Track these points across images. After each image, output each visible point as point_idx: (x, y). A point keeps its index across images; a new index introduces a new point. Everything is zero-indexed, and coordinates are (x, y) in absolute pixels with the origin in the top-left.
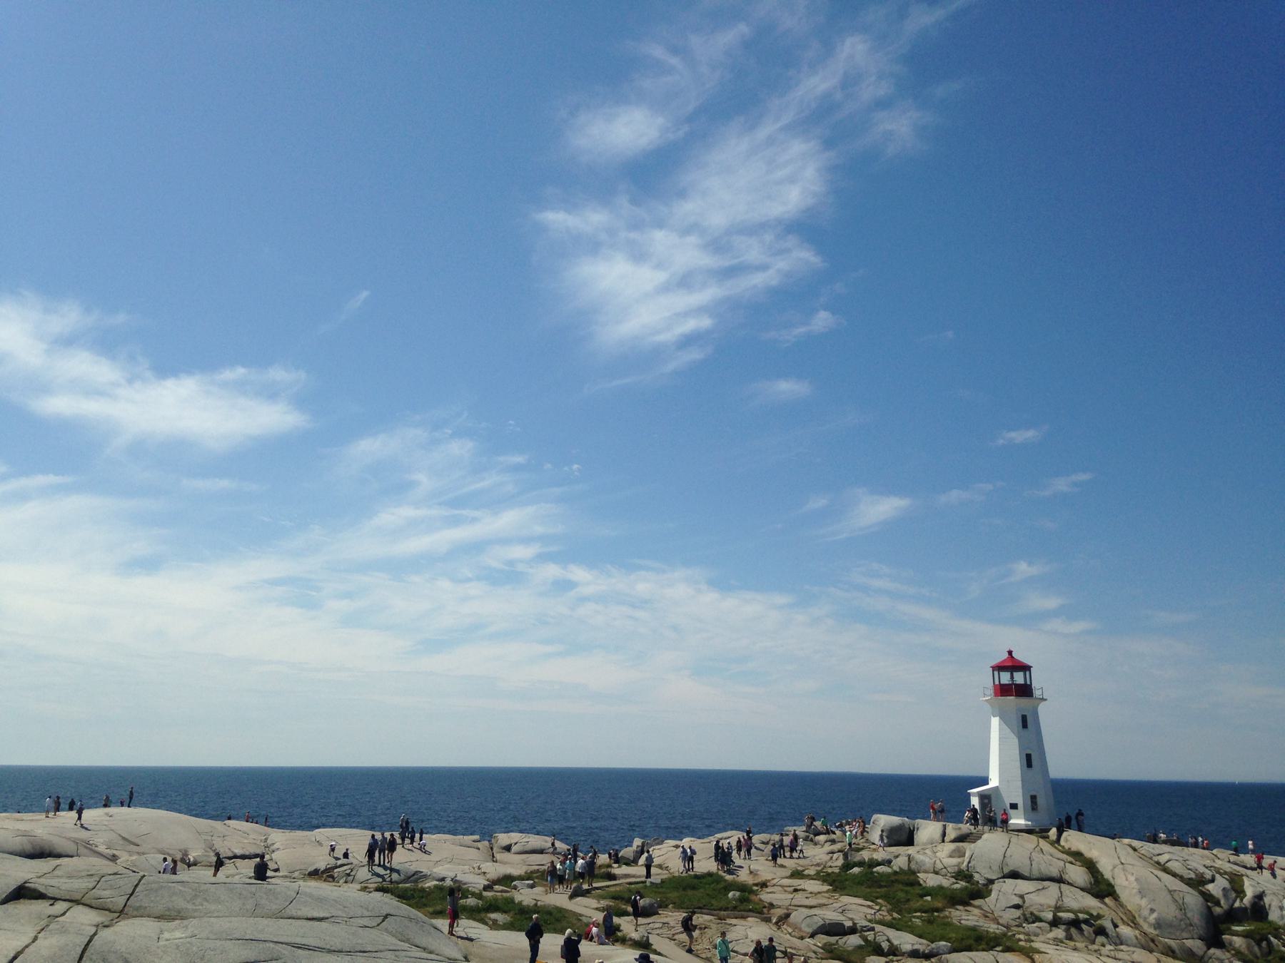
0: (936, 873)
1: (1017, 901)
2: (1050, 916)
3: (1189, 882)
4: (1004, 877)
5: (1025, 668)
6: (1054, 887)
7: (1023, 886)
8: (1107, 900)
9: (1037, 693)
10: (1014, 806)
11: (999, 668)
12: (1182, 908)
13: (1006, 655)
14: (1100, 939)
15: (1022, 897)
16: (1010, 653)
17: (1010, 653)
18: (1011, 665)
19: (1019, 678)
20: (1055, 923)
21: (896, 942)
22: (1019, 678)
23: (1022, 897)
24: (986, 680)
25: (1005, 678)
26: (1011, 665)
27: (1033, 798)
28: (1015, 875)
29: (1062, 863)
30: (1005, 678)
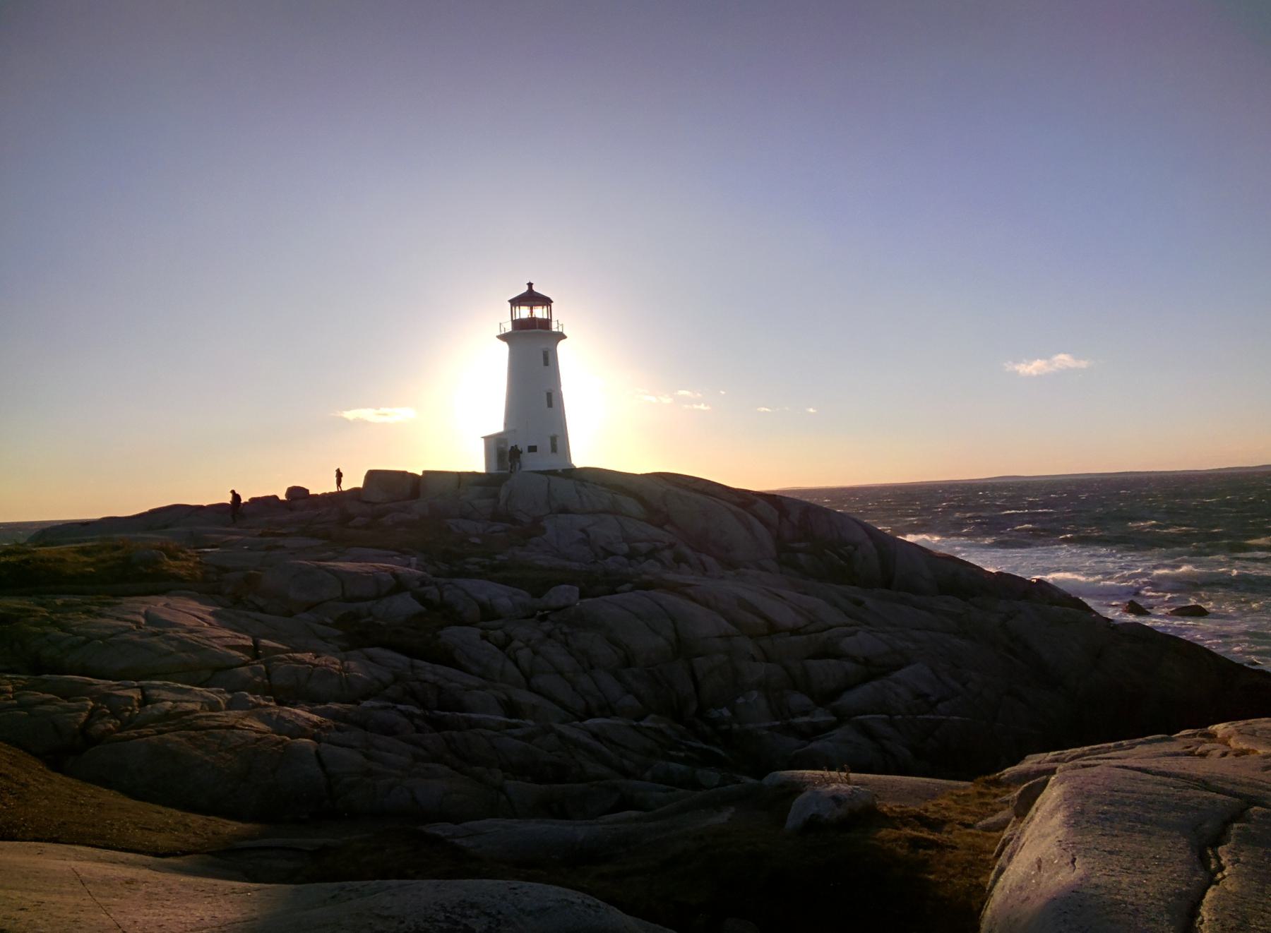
3: (738, 505)
5: (546, 302)
9: (554, 328)
11: (516, 302)
13: (526, 289)
15: (583, 530)
16: (530, 285)
17: (530, 285)
18: (531, 298)
19: (540, 313)
21: (483, 597)
22: (540, 313)
23: (583, 530)
25: (524, 312)
26: (531, 298)
28: (564, 510)
30: (524, 312)
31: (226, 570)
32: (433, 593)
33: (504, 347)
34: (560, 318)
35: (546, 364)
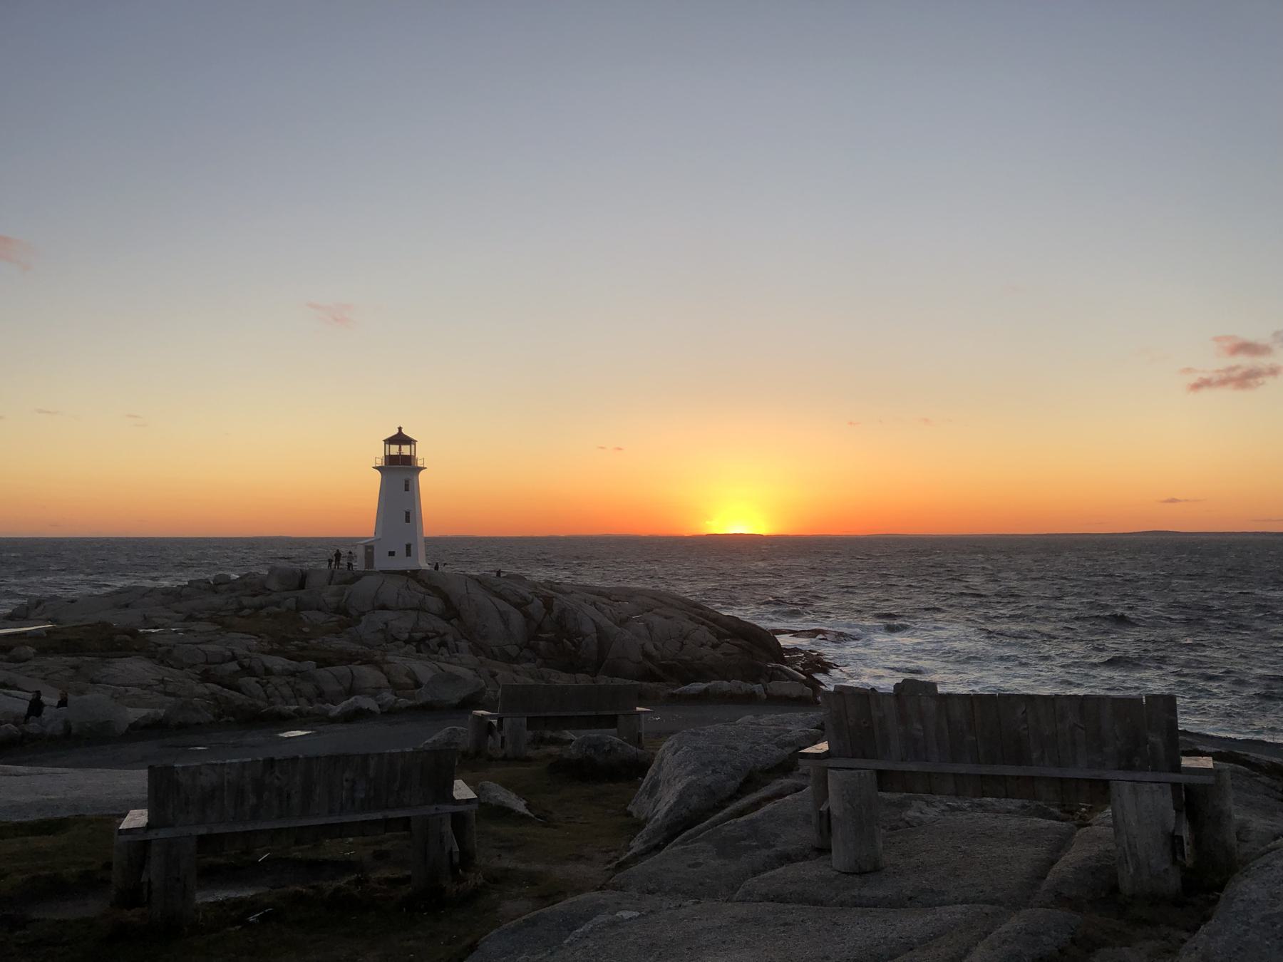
0: (319, 610)
1: (381, 626)
2: (406, 636)
4: (374, 609)
6: (413, 614)
7: (388, 615)
8: (454, 621)
10: (392, 554)
12: (506, 622)
13: (396, 431)
14: (443, 650)
16: (400, 429)
17: (400, 429)
18: (400, 439)
19: (406, 450)
20: (407, 642)
21: (268, 665)
22: (406, 450)
23: (386, 624)
24: (377, 453)
25: (394, 450)
26: (400, 439)
27: (408, 547)
28: (384, 607)
29: (421, 596)
30: (394, 450)
31: (160, 645)
32: (246, 662)
33: (378, 475)
34: (422, 454)
35: (407, 489)
